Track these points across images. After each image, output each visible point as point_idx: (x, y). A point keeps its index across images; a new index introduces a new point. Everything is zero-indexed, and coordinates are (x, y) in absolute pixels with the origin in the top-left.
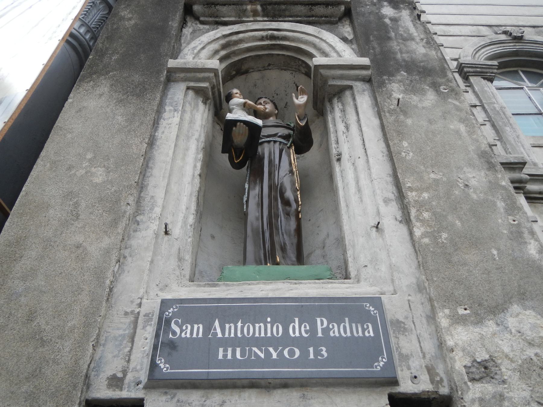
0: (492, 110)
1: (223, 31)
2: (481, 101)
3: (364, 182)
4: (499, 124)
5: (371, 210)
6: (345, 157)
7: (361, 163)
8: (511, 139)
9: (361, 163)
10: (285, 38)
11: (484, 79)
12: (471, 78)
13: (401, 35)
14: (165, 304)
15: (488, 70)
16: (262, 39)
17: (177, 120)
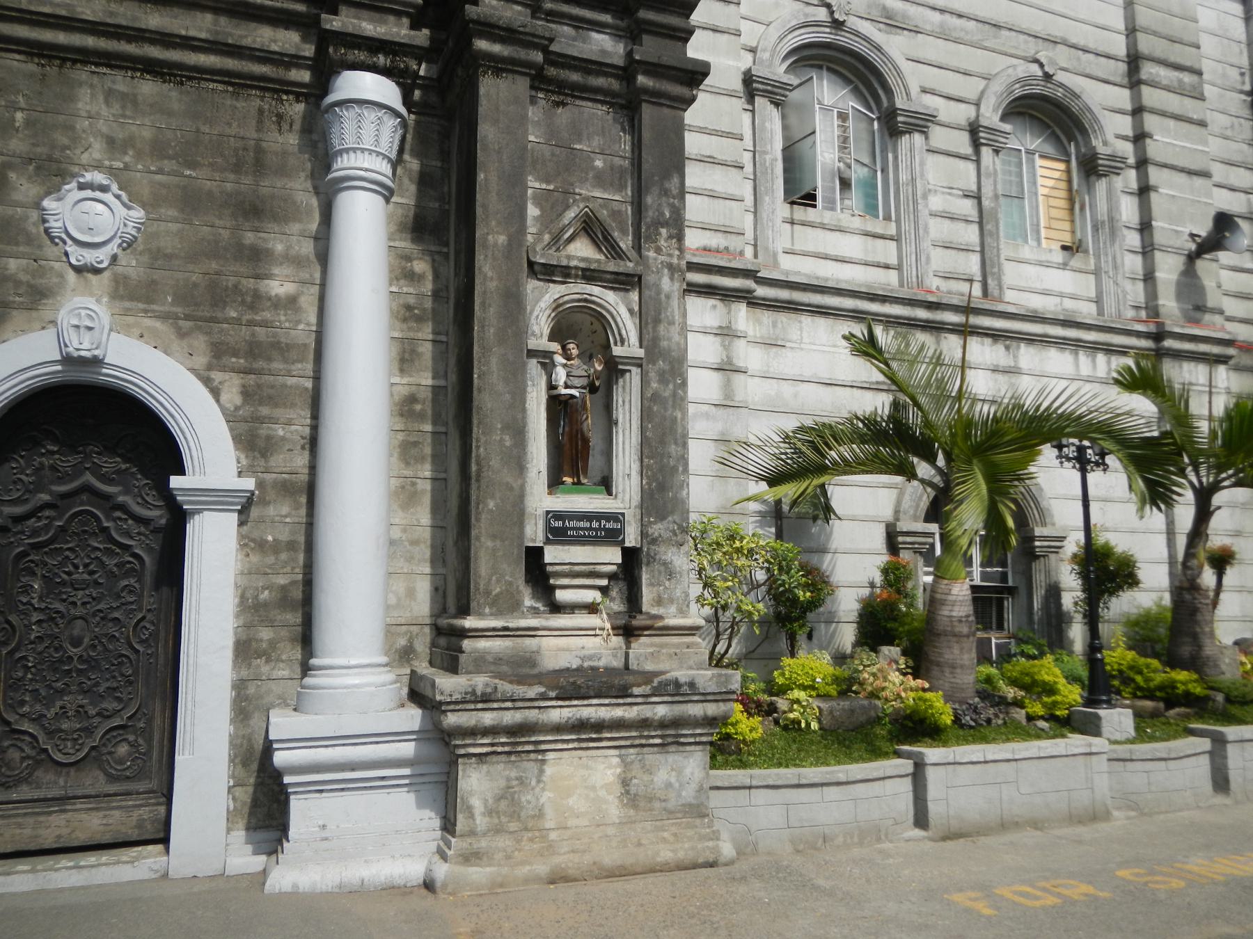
0: (761, 164)
1: (554, 294)
2: (755, 146)
3: (627, 446)
4: (761, 189)
5: (627, 465)
6: (620, 424)
7: (627, 432)
8: (764, 216)
9: (627, 432)
10: (593, 302)
11: (772, 102)
12: (756, 98)
13: (667, 317)
14: (548, 512)
15: (780, 91)
16: (579, 300)
17: (535, 393)
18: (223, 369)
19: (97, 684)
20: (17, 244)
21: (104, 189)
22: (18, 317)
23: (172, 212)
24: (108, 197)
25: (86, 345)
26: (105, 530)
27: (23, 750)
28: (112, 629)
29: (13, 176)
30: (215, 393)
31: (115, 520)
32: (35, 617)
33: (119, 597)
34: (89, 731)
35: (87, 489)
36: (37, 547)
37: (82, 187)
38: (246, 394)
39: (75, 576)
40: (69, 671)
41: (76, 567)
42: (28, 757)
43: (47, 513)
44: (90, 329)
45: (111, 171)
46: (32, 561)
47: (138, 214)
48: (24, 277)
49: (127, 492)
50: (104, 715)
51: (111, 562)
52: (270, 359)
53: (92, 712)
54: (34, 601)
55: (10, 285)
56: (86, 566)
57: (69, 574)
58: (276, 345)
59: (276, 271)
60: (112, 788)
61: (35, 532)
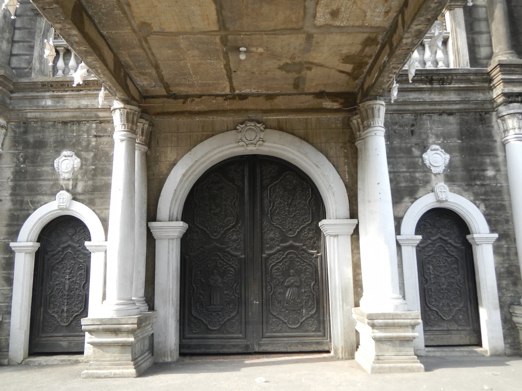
18: (478, 200)
19: (451, 297)
20: (418, 169)
21: (437, 150)
22: (421, 191)
23: (457, 154)
24: (438, 152)
25: (444, 197)
26: (447, 251)
27: (434, 316)
28: (453, 280)
29: (413, 149)
30: (478, 207)
31: (448, 247)
32: (432, 276)
33: (452, 270)
34: (450, 310)
35: (440, 238)
36: (429, 256)
37: (432, 150)
38: (486, 207)
39: (440, 264)
40: (443, 293)
41: (440, 261)
42: (436, 318)
43: (431, 246)
44: (444, 192)
45: (439, 144)
46: (429, 260)
47: (448, 156)
48: (421, 178)
49: (450, 239)
50: (454, 306)
51: (449, 260)
52: (490, 196)
53: (451, 305)
54: (431, 272)
55: (418, 181)
56: (442, 261)
57: (438, 264)
58: (492, 191)
59: (488, 168)
60: (460, 328)
61: (428, 252)
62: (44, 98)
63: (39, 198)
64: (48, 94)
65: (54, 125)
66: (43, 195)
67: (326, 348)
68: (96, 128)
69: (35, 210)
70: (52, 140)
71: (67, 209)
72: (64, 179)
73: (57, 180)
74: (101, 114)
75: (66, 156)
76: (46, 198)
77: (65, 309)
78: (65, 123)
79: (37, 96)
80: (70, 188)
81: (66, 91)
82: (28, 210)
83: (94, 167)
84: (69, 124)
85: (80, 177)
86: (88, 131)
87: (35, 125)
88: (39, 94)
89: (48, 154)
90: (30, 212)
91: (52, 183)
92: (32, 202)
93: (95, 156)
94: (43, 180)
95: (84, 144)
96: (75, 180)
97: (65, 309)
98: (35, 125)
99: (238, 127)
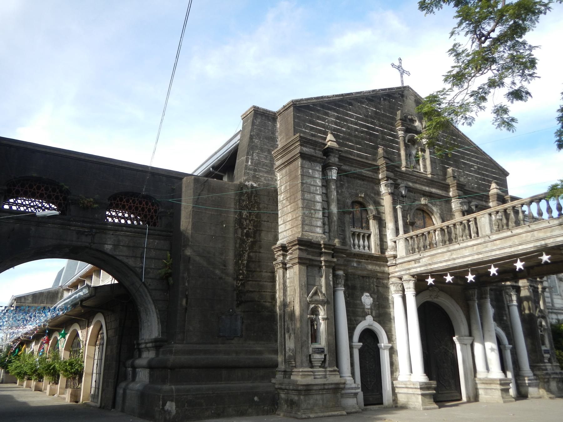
62: (353, 261)
63: (358, 318)
64: (356, 260)
65: (358, 278)
66: (359, 316)
67: (458, 398)
68: (376, 282)
69: (357, 325)
70: (359, 286)
71: (371, 325)
72: (367, 309)
73: (364, 308)
74: (379, 275)
75: (367, 296)
76: (360, 318)
77: (369, 380)
78: (363, 277)
79: (351, 260)
80: (370, 313)
81: (362, 259)
82: (354, 324)
83: (378, 303)
84: (365, 278)
85: (373, 308)
86: (373, 283)
87: (351, 276)
88: (351, 259)
89: (358, 294)
90: (355, 326)
91: (362, 310)
92: (355, 320)
93: (378, 297)
94: (358, 308)
95: (372, 290)
96: (371, 309)
97: (369, 380)
98: (351, 276)
99: (430, 289)
